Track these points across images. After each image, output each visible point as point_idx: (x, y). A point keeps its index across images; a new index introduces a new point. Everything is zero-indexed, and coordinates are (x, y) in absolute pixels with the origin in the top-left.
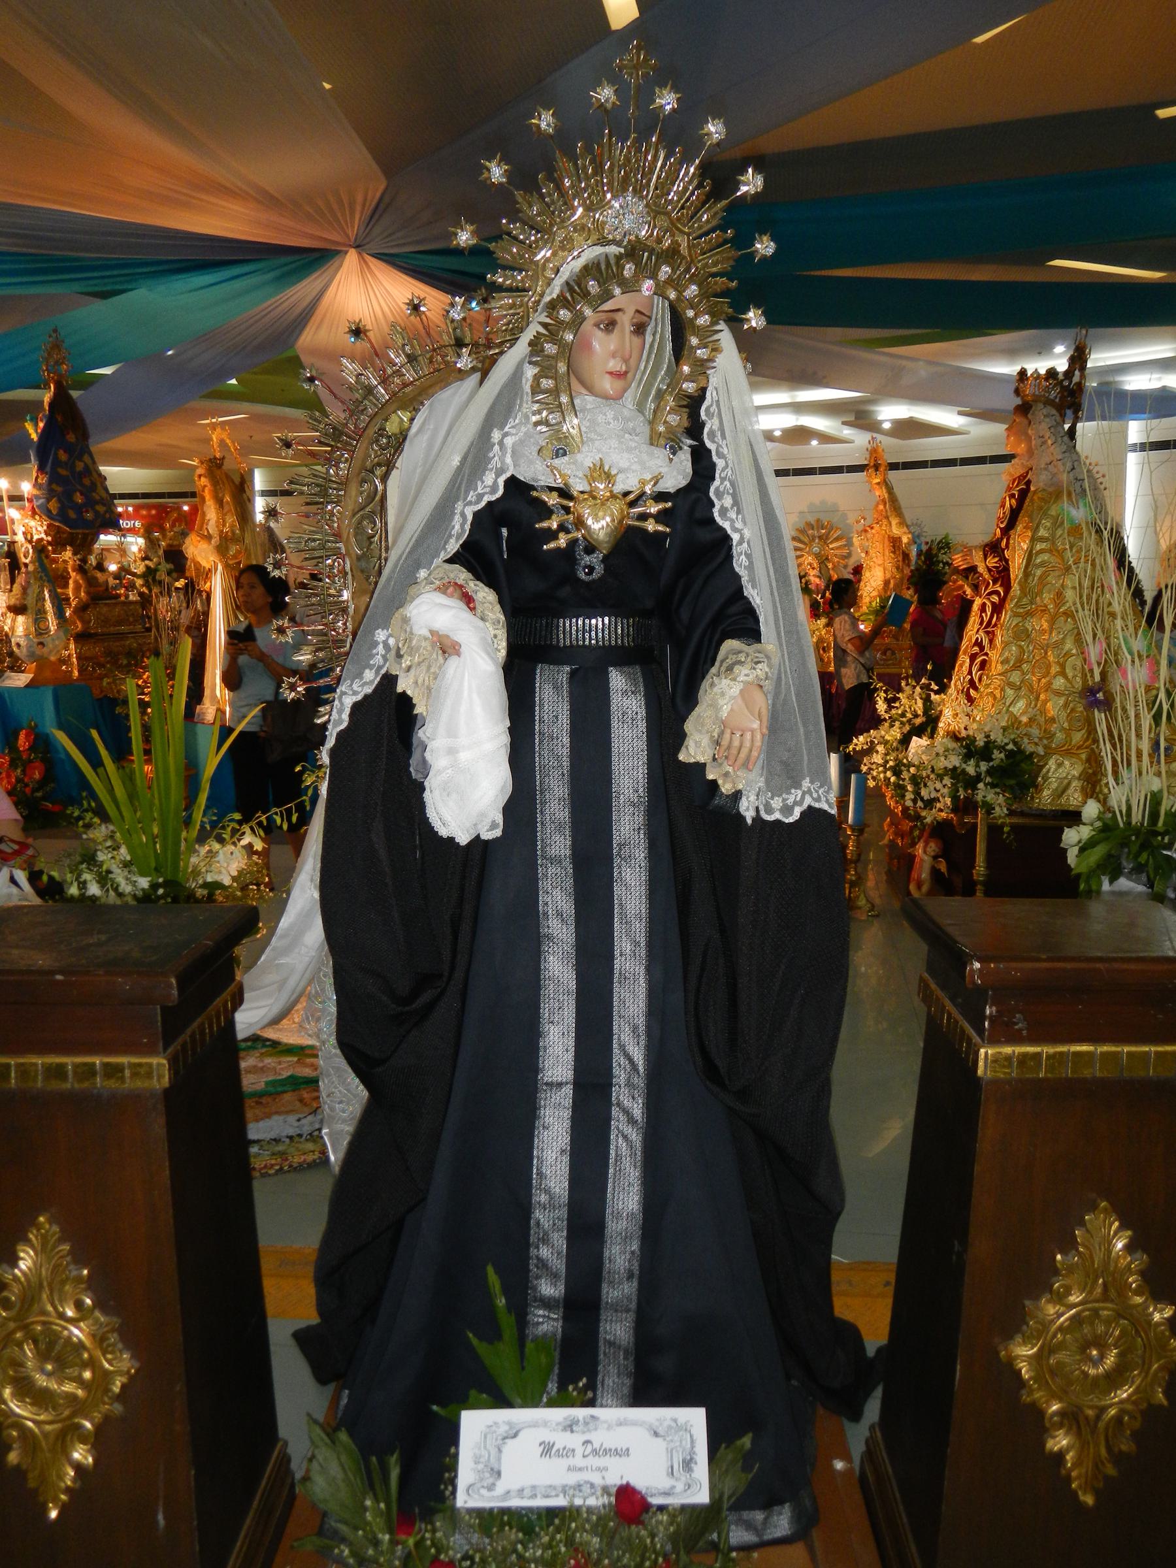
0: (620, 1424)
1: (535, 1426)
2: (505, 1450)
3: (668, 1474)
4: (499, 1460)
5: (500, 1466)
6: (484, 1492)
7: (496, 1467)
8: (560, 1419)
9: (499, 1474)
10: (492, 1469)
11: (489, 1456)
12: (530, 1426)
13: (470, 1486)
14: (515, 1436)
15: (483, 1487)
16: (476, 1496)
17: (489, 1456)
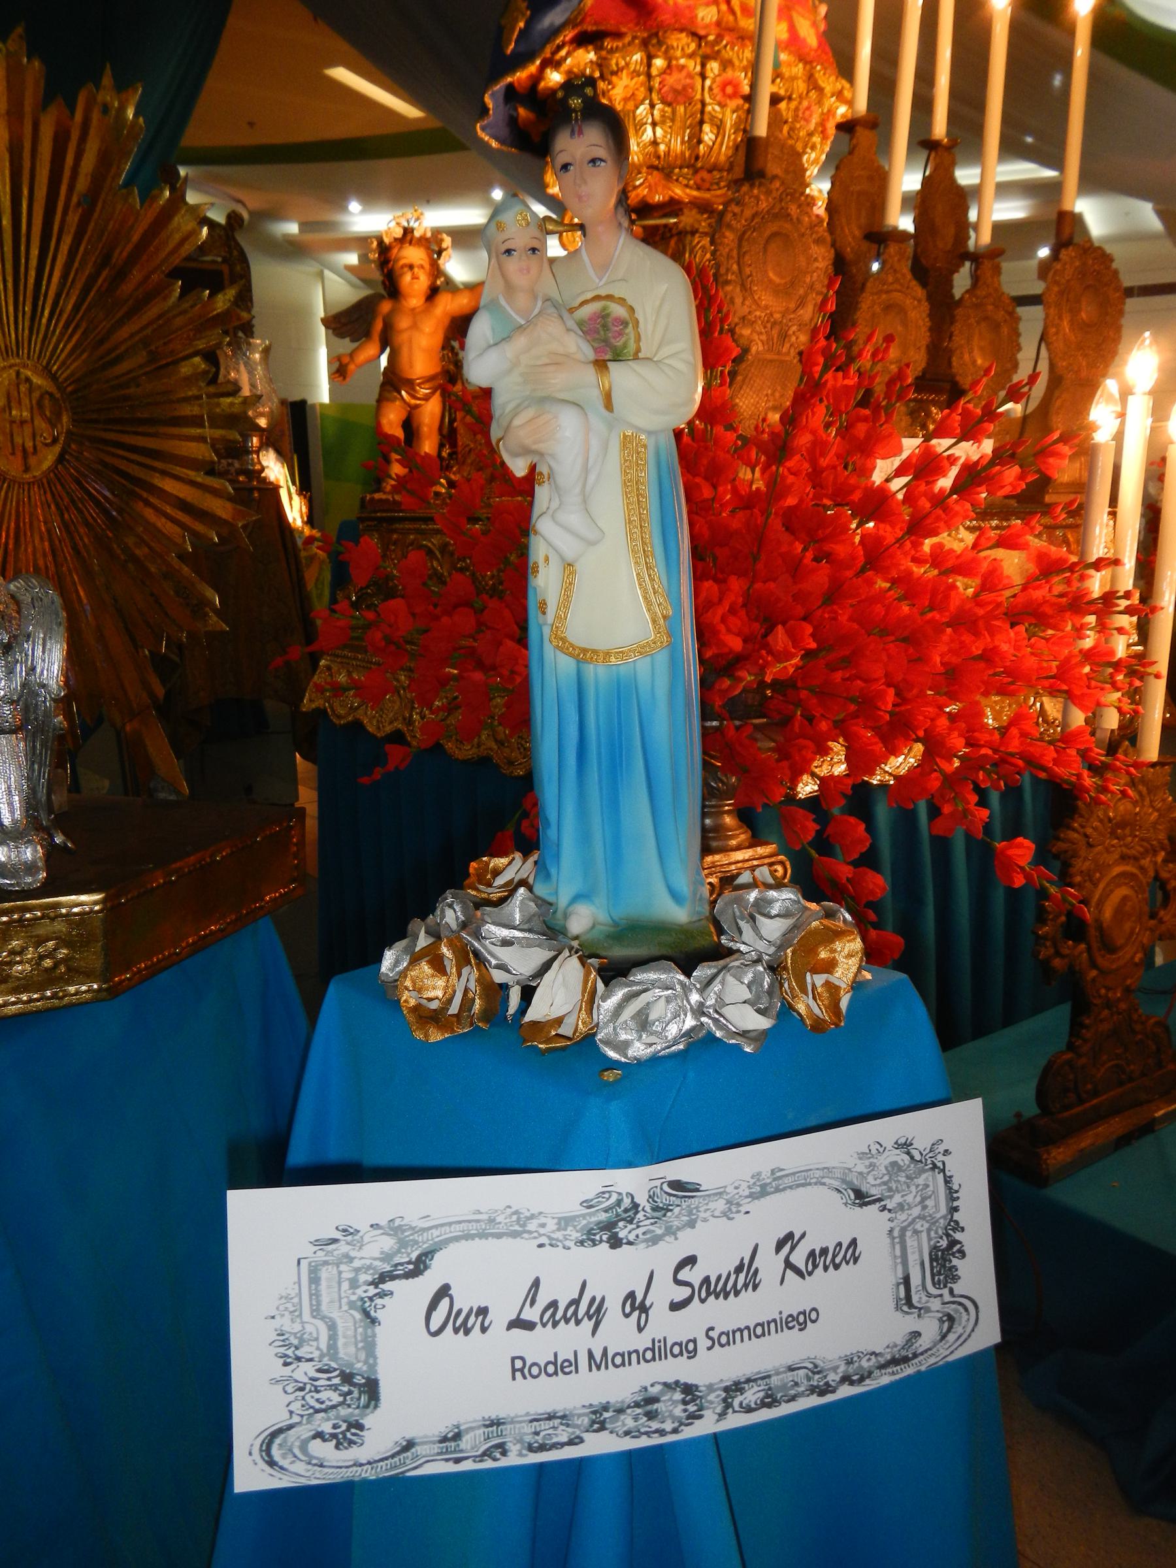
0: (762, 1191)
1: (483, 1235)
2: (387, 1311)
3: (898, 1308)
4: (370, 1347)
5: (373, 1367)
6: (323, 1450)
7: (359, 1365)
8: (573, 1207)
9: (371, 1389)
10: (347, 1378)
11: (333, 1337)
12: (468, 1237)
13: (274, 1435)
14: (418, 1267)
15: (319, 1435)
16: (300, 1467)
17: (333, 1337)
